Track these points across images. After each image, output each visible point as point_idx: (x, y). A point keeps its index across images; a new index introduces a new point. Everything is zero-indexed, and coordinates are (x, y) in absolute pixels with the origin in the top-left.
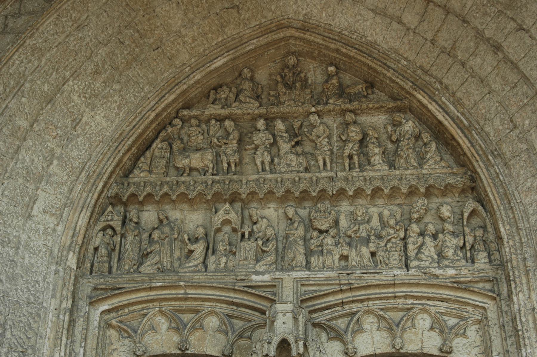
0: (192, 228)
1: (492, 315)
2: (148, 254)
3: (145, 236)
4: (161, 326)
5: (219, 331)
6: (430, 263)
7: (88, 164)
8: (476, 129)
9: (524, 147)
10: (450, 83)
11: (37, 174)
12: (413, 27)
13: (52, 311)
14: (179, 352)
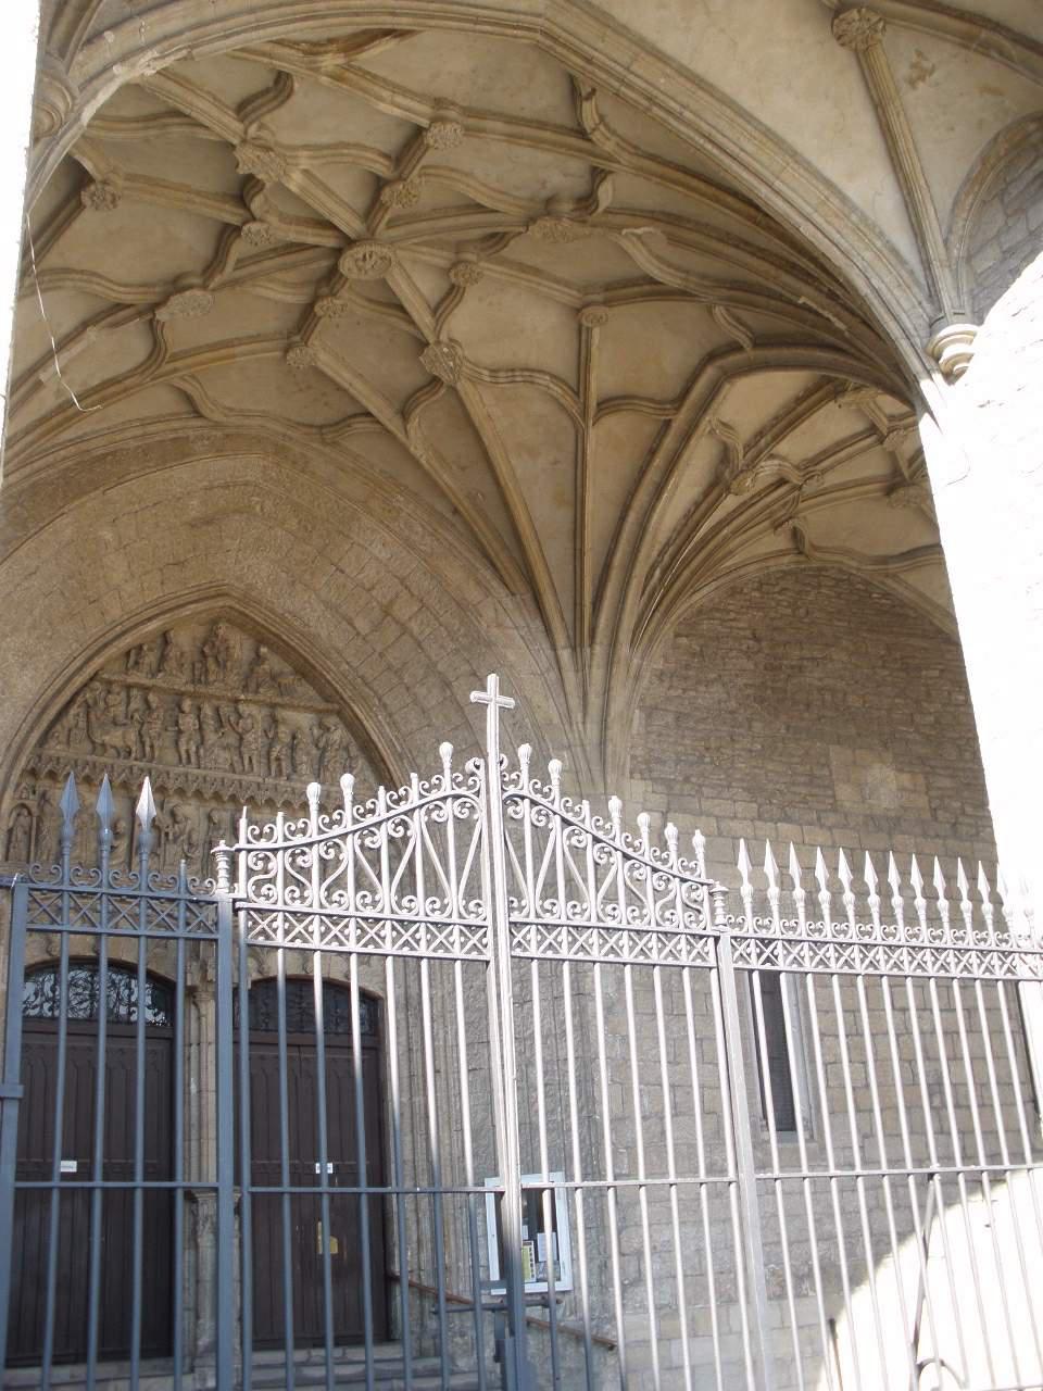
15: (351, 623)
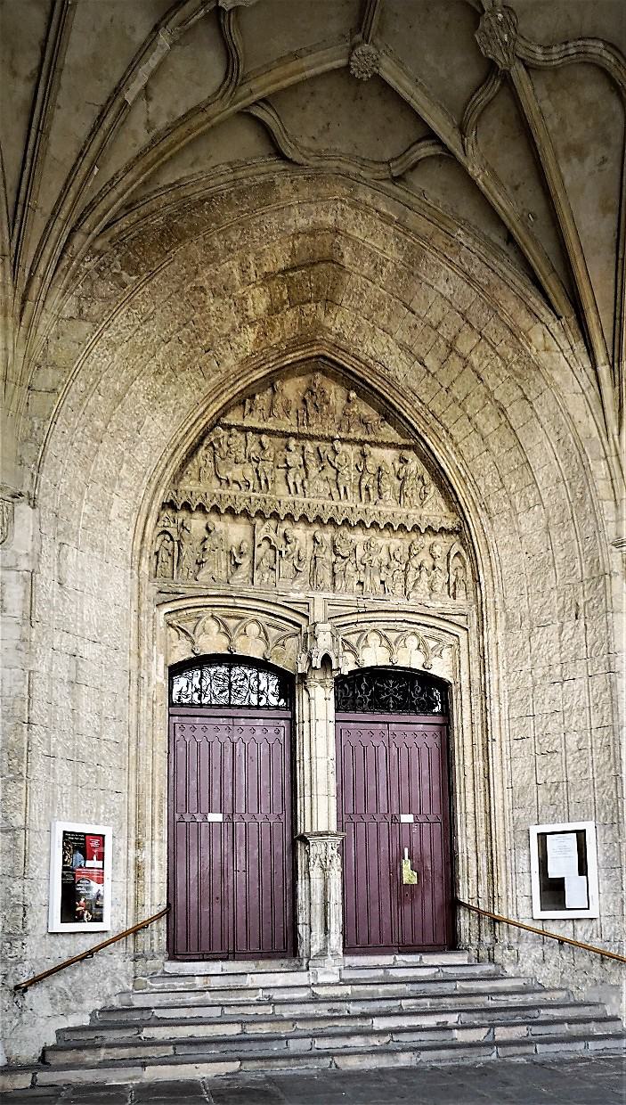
0: (235, 540)
1: (463, 642)
2: (202, 562)
9: (507, 506)
12: (432, 372)
14: (228, 653)
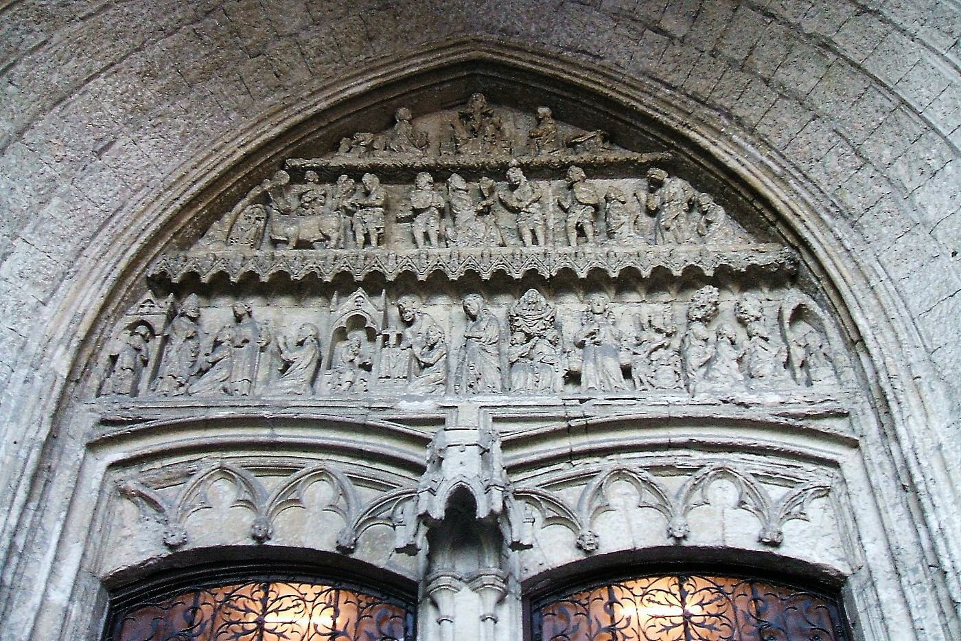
3: (206, 343)
4: (221, 497)
5: (333, 507)
6: (732, 386)
7: (117, 217)
8: (795, 178)
10: (747, 113)
11: (18, 212)
13: (8, 445)
15: (659, 31)
